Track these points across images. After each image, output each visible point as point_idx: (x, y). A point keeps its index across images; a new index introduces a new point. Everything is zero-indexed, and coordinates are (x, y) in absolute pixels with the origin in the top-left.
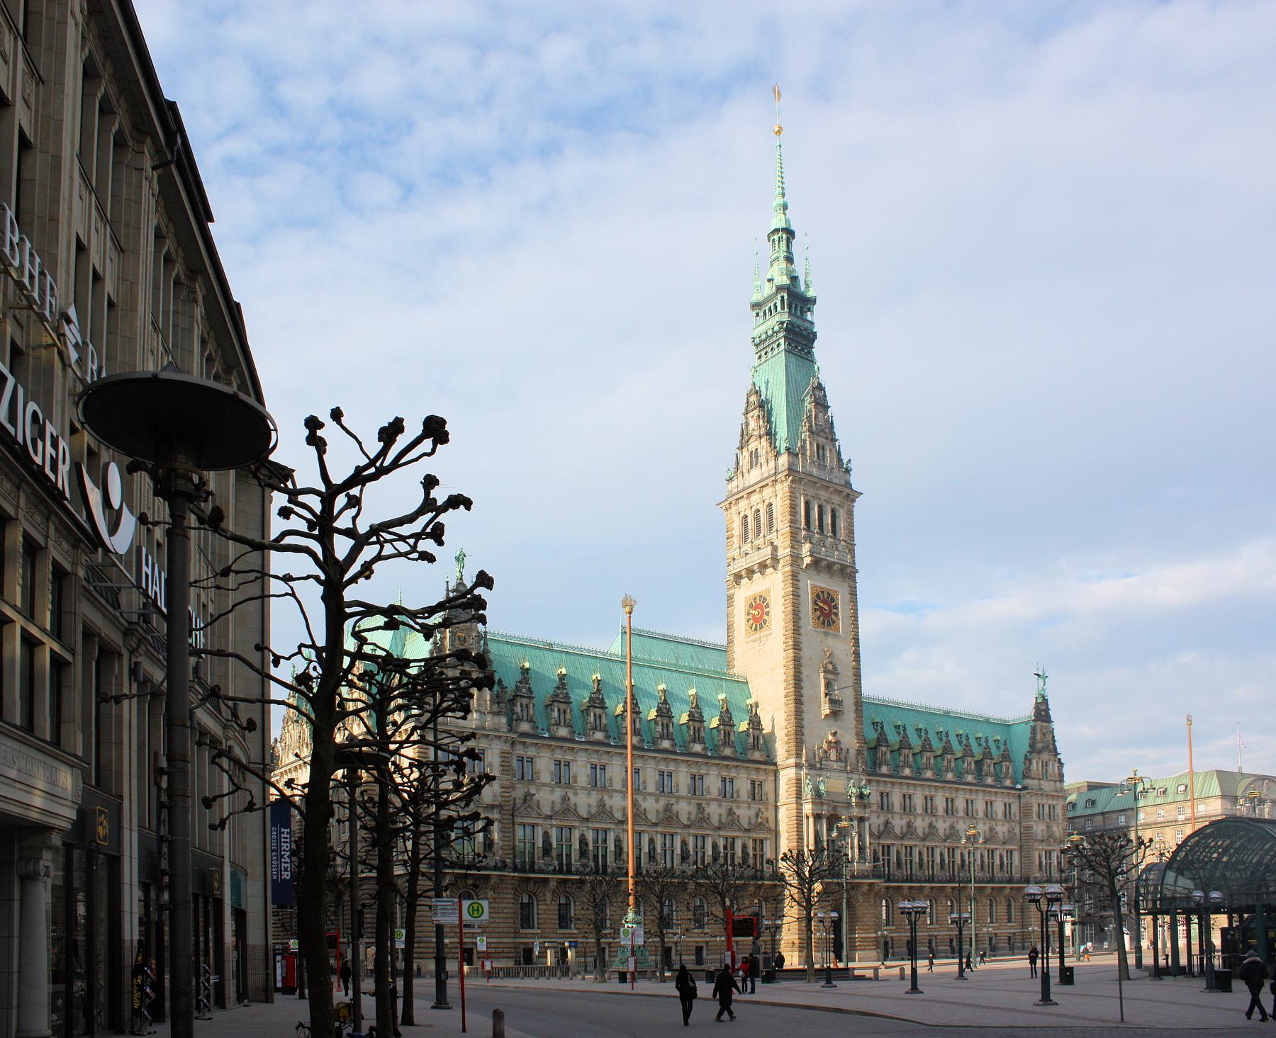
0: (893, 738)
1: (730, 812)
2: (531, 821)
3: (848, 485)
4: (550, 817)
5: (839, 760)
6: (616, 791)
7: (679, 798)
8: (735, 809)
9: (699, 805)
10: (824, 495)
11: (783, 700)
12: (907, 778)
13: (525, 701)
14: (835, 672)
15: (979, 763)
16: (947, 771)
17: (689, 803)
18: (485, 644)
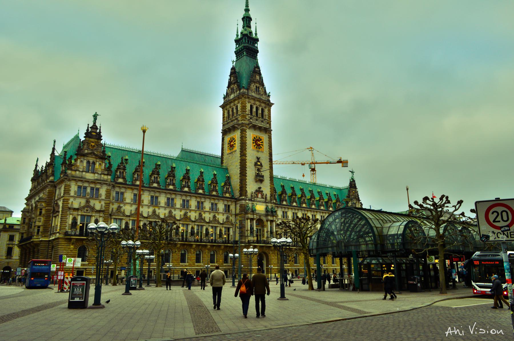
0: (289, 192)
1: (214, 217)
2: (120, 217)
3: (269, 101)
4: (129, 216)
5: (263, 198)
6: (162, 207)
7: (190, 211)
8: (217, 215)
9: (200, 213)
10: (258, 103)
11: (239, 175)
12: (294, 206)
13: (122, 171)
14: (261, 165)
15: (327, 203)
16: (312, 205)
17: (195, 212)
18: (104, 148)
